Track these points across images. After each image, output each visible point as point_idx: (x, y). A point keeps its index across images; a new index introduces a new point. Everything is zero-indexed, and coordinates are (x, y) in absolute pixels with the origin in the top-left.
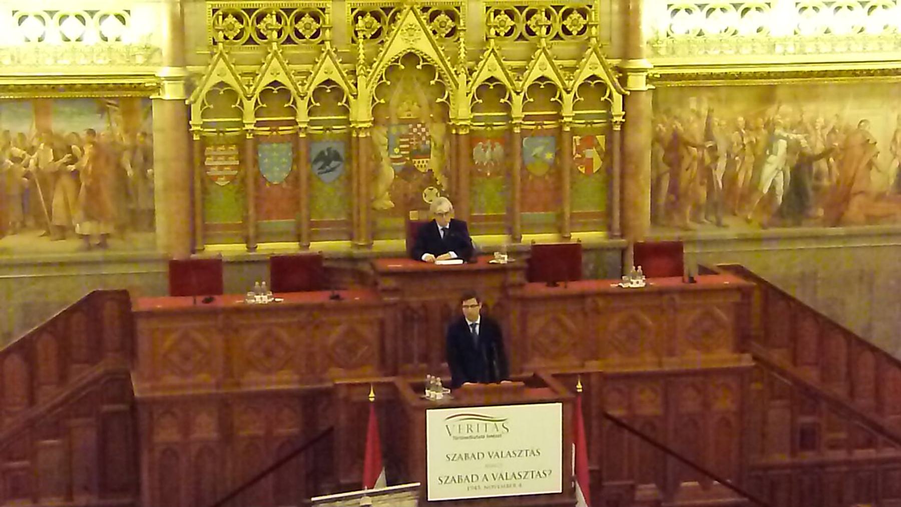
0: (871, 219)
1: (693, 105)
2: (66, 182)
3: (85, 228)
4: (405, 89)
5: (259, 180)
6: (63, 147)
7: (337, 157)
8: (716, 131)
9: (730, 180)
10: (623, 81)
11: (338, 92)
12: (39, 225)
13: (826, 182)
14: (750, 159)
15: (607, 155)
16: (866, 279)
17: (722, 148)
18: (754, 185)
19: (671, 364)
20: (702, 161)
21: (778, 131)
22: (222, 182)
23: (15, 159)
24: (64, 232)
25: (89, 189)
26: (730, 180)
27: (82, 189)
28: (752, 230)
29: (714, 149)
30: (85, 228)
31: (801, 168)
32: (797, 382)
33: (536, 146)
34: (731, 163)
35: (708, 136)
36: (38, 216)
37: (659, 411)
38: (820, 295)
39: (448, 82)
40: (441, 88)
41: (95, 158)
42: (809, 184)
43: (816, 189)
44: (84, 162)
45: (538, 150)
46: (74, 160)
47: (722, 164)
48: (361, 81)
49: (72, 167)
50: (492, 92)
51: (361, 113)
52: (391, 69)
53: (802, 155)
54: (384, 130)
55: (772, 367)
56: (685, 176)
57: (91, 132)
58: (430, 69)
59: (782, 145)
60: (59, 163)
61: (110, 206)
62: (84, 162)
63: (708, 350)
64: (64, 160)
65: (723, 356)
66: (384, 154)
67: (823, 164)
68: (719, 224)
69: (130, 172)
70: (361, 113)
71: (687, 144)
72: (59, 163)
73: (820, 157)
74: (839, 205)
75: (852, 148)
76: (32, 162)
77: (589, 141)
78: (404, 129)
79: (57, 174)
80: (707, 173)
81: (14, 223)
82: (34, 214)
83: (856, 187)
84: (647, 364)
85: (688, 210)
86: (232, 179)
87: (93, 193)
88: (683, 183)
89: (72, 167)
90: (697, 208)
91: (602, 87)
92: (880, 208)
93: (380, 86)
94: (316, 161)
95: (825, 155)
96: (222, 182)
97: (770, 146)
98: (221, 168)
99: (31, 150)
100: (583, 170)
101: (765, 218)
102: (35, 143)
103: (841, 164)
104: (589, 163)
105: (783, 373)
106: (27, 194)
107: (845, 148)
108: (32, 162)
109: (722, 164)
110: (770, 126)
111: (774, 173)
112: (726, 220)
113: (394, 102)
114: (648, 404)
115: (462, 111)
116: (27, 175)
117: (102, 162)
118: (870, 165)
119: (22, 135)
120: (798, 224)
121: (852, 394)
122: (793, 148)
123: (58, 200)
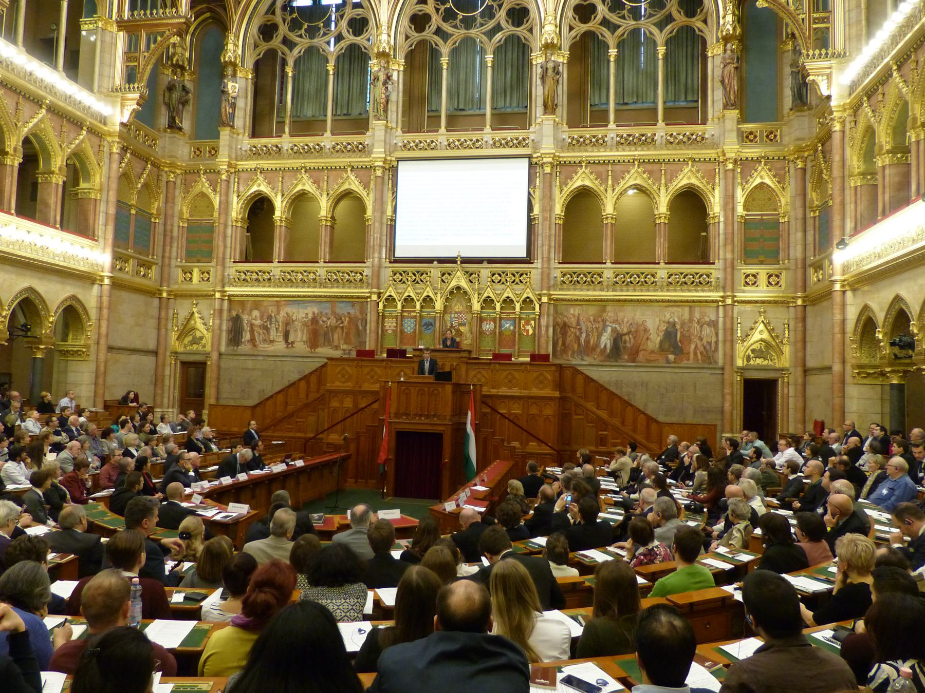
0: (648, 361)
1: (572, 311)
2: (339, 330)
3: (344, 347)
5: (402, 331)
6: (339, 318)
7: (431, 324)
8: (581, 322)
9: (587, 342)
10: (540, 299)
11: (431, 300)
13: (628, 345)
14: (596, 334)
15: (534, 329)
16: (645, 385)
17: (584, 329)
18: (597, 345)
19: (525, 393)
20: (575, 334)
21: (608, 323)
24: (337, 348)
26: (587, 342)
28: (595, 363)
29: (580, 329)
30: (344, 347)
31: (617, 339)
32: (598, 417)
34: (588, 335)
35: (578, 324)
36: (329, 341)
37: (520, 412)
38: (624, 390)
39: (472, 297)
40: (469, 299)
41: (349, 322)
42: (621, 345)
43: (624, 347)
44: (346, 323)
46: (342, 322)
47: (584, 335)
48: (439, 295)
50: (488, 302)
51: (439, 305)
52: (451, 293)
53: (618, 333)
55: (587, 410)
56: (568, 340)
58: (465, 293)
59: (609, 329)
61: (353, 339)
62: (346, 323)
63: (541, 389)
65: (548, 392)
67: (627, 337)
68: (582, 359)
70: (439, 305)
71: (569, 327)
73: (625, 334)
74: (634, 354)
75: (639, 331)
77: (528, 323)
79: (336, 327)
80: (578, 339)
82: (328, 342)
83: (641, 348)
84: (515, 392)
85: (570, 353)
86: (393, 331)
87: (348, 334)
88: (568, 342)
90: (573, 352)
91: (532, 301)
92: (652, 357)
93: (447, 299)
95: (628, 334)
96: (390, 332)
97: (605, 327)
99: (329, 319)
101: (602, 358)
103: (635, 338)
104: (528, 331)
105: (593, 412)
106: (326, 334)
107: (636, 332)
109: (584, 335)
110: (604, 321)
111: (606, 340)
112: (585, 358)
114: (516, 409)
115: (476, 306)
118: (648, 339)
120: (616, 361)
121: (623, 423)
122: (614, 330)
123: (336, 336)
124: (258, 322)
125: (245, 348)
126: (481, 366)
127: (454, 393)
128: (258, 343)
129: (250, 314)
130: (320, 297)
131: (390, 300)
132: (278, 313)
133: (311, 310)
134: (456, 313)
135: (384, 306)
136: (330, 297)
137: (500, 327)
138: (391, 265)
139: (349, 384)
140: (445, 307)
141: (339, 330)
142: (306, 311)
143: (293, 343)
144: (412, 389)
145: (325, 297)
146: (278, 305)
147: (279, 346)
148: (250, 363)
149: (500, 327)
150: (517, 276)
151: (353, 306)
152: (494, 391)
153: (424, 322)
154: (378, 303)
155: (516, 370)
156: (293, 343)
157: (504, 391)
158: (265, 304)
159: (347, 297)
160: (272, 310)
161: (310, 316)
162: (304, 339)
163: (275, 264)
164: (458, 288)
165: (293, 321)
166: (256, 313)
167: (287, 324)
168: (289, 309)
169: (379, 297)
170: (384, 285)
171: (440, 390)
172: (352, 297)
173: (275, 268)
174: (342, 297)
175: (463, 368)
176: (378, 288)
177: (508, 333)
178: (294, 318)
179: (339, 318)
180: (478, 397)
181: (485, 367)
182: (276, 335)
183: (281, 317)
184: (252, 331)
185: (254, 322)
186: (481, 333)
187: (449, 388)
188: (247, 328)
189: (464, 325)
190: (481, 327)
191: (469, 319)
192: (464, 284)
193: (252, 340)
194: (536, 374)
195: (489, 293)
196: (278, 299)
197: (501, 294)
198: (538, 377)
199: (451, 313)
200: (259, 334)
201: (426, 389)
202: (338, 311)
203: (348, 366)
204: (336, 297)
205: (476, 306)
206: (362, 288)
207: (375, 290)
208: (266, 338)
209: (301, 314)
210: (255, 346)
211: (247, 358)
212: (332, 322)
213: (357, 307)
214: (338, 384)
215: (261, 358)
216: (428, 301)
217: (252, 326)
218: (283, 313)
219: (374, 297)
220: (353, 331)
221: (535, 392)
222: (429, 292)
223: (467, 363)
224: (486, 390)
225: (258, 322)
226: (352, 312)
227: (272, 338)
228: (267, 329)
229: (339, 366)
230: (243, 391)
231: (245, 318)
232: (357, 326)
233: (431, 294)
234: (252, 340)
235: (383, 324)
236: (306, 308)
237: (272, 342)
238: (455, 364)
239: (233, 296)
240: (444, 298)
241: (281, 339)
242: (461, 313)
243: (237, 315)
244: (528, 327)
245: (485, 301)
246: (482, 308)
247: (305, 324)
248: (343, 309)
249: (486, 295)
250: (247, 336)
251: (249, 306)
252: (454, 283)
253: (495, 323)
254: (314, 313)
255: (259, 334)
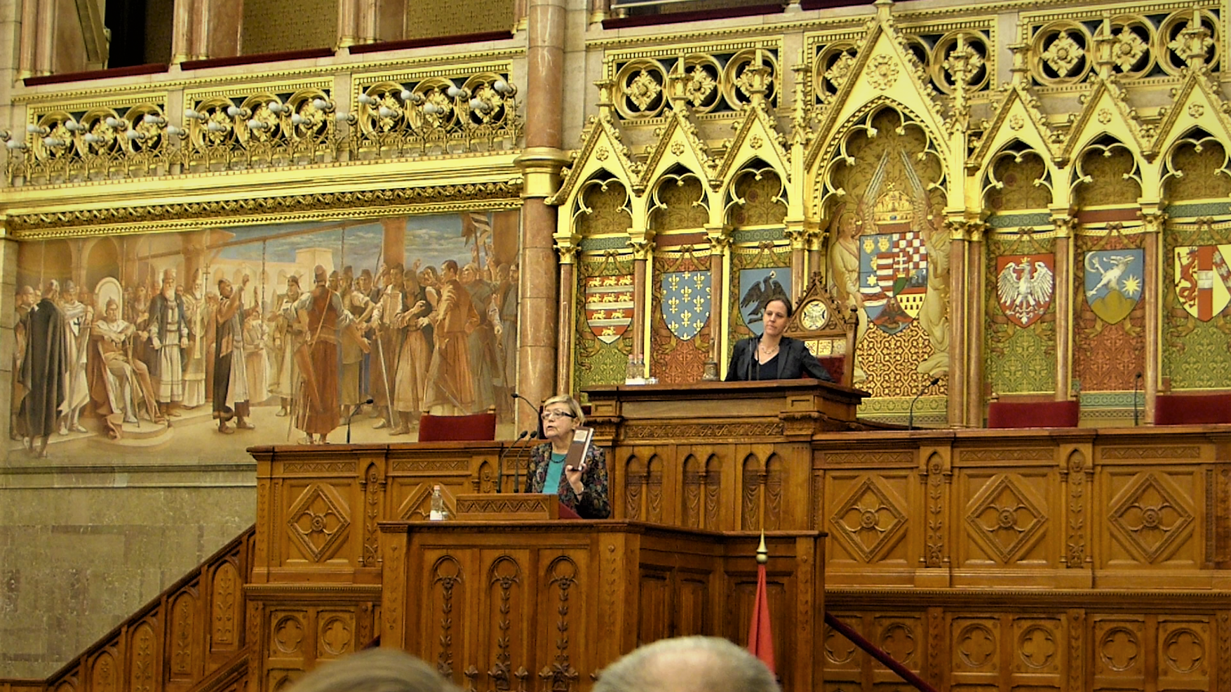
2: (416, 343)
4: (888, 178)
12: (381, 411)
19: (1076, 581)
22: (608, 337)
23: (357, 310)
25: (444, 355)
27: (436, 356)
33: (1107, 267)
40: (935, 163)
41: (454, 307)
44: (441, 310)
45: (1112, 276)
46: (428, 310)
48: (798, 153)
49: (424, 321)
52: (856, 138)
54: (853, 246)
57: (452, 266)
58: (917, 132)
60: (408, 315)
61: (469, 382)
62: (441, 310)
64: (414, 310)
65: (1185, 574)
66: (851, 287)
69: (498, 328)
72: (408, 315)
76: (376, 313)
77: (1205, 259)
78: (884, 245)
79: (405, 332)
81: (347, 407)
86: (624, 332)
87: (449, 361)
89: (424, 321)
93: (839, 169)
94: (746, 302)
96: (608, 337)
98: (609, 314)
99: (376, 296)
100: (1194, 312)
102: (381, 286)
106: (366, 362)
108: (376, 313)
113: (870, 196)
116: (369, 334)
117: (464, 310)
119: (366, 273)
124: (116, 329)
125: (72, 440)
126: (877, 460)
127: (651, 571)
128: (115, 419)
129: (88, 297)
130: (338, 201)
131: (602, 190)
132: (190, 288)
133: (312, 261)
134: (885, 231)
135: (582, 221)
136: (376, 199)
137: (1080, 283)
138: (613, 35)
139: (340, 564)
140: (833, 205)
141: (416, 343)
142: (291, 271)
143: (242, 409)
144: (465, 556)
145: (357, 200)
146: (188, 249)
147: (195, 428)
148: (80, 505)
149: (1080, 283)
150: (1155, 34)
151: (469, 232)
152: (932, 578)
153: (750, 279)
154: (554, 208)
155: (1031, 472)
156: (242, 409)
157: (981, 574)
158: (143, 249)
159: (439, 195)
160: (167, 270)
161: (307, 288)
162: (286, 390)
163: (175, 73)
164: (885, 114)
165: (245, 315)
166: (110, 290)
167: (222, 330)
168: (225, 266)
169: (558, 182)
170: (577, 134)
171: (580, 557)
172: (459, 194)
173: (172, 93)
174: (419, 196)
175: (797, 465)
176: (559, 145)
177: (1113, 313)
178: (247, 302)
179: (415, 291)
180: (804, 597)
181: (891, 459)
182: (182, 381)
183: (199, 307)
184: (96, 368)
185: (103, 327)
186: (994, 321)
187: (614, 547)
188: (77, 356)
189: (918, 286)
190: (992, 288)
191: (939, 256)
192: (908, 93)
193: (97, 407)
194: (1126, 487)
195: (1022, 124)
196: (185, 224)
197: (1072, 129)
198: (1131, 503)
199: (860, 234)
200: (121, 378)
201: (523, 557)
202: (410, 258)
203: (336, 482)
204: (397, 198)
205: (965, 195)
206: (494, 148)
207: (543, 152)
208: (146, 392)
209: (274, 280)
210: (106, 430)
211: (73, 481)
212: (389, 308)
213: (485, 235)
214: (297, 564)
215: (121, 481)
216: (756, 181)
217: (96, 343)
218: (206, 285)
219: (539, 184)
220: (469, 345)
221: (1124, 574)
222: (762, 142)
223: (815, 448)
224: (848, 573)
225: (116, 329)
226: (465, 258)
227: (165, 394)
228: (147, 355)
229: (301, 483)
230: (58, 624)
231: (71, 310)
232: (484, 318)
233: (767, 154)
234: (97, 407)
235: (582, 305)
236: (288, 256)
237: (167, 408)
238: (763, 453)
239: (24, 225)
240: (823, 168)
241: (198, 395)
242: (903, 230)
243: (46, 305)
244: (1211, 279)
245: (1003, 163)
246: (992, 198)
247: (288, 327)
248: (433, 249)
249: (1004, 136)
250: (78, 391)
251: (85, 258)
252: (862, 96)
253: (1053, 266)
254: (320, 277)
255: (121, 378)
